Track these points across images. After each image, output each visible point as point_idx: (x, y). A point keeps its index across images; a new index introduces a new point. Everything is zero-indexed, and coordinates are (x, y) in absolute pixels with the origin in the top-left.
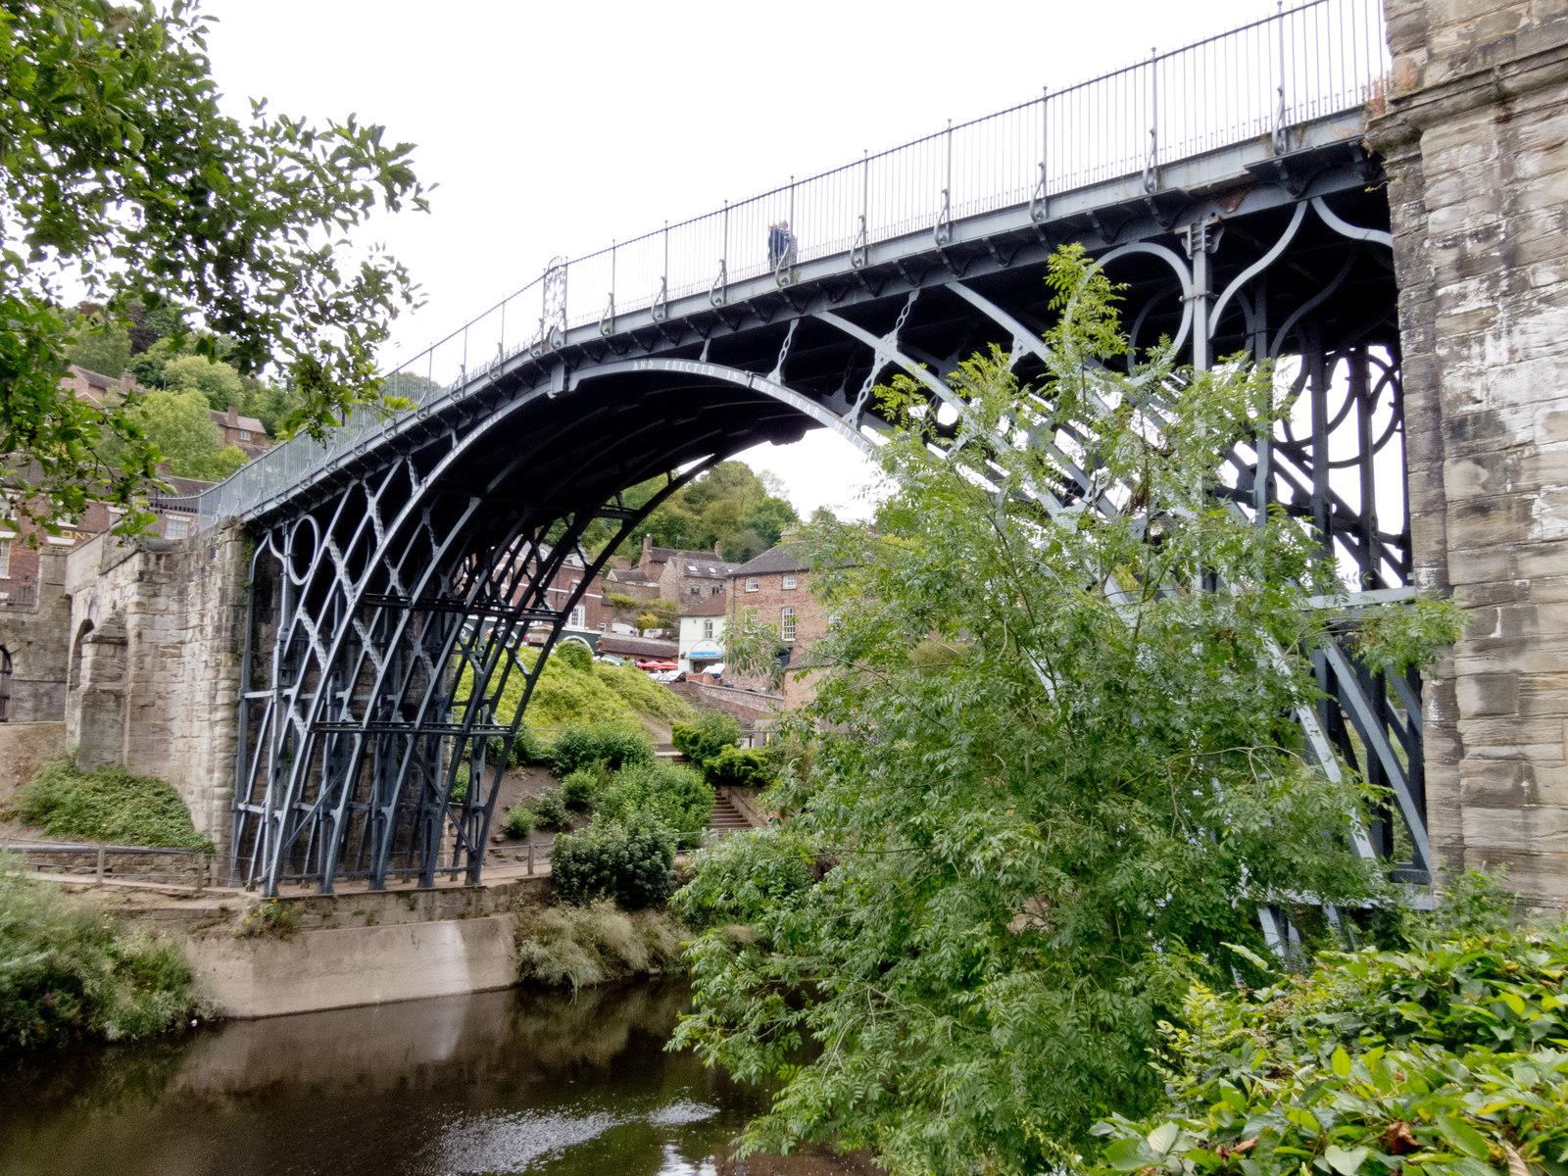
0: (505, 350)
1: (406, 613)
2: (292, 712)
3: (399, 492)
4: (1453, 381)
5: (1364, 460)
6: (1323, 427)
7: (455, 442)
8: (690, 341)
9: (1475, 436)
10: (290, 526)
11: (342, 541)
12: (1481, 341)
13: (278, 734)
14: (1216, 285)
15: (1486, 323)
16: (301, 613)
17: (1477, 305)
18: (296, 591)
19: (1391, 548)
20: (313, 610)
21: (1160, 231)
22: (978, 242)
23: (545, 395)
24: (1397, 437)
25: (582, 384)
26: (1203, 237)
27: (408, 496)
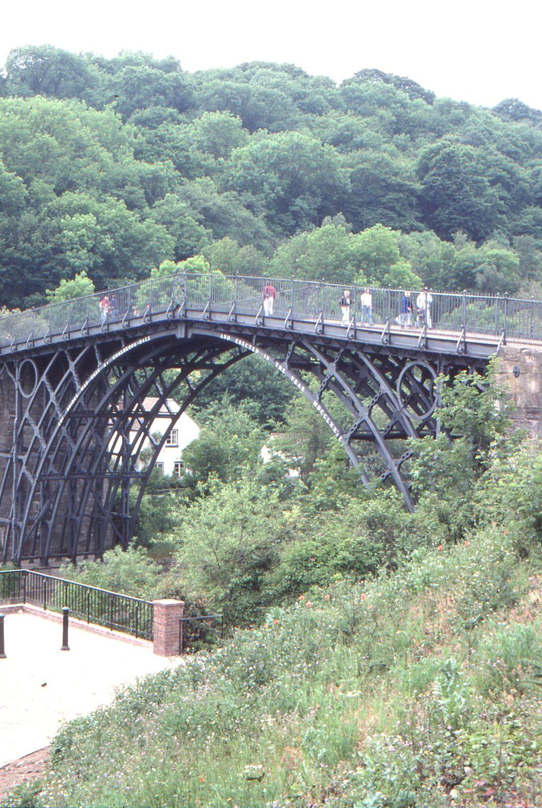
7: (123, 345)
10: (19, 362)
11: (54, 378)
23: (174, 336)
25: (194, 336)
26: (442, 367)
27: (95, 368)
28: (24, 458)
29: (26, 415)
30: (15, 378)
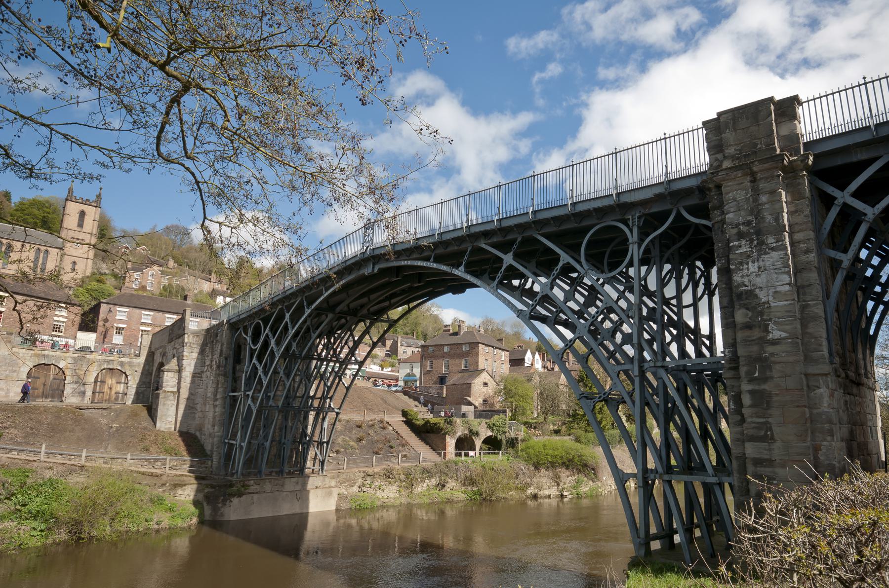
0: (347, 255)
1: (299, 361)
2: (249, 401)
3: (300, 310)
4: (737, 278)
5: (695, 305)
6: (680, 291)
8: (425, 254)
9: (746, 299)
10: (251, 324)
11: (274, 330)
12: (747, 263)
13: (243, 410)
14: (641, 241)
15: (749, 257)
16: (254, 361)
17: (745, 250)
18: (252, 352)
19: (705, 340)
20: (260, 360)
21: (619, 217)
22: (547, 219)
24: (706, 297)
25: (379, 269)
28: (250, 393)
29: (254, 361)
30: (247, 334)
